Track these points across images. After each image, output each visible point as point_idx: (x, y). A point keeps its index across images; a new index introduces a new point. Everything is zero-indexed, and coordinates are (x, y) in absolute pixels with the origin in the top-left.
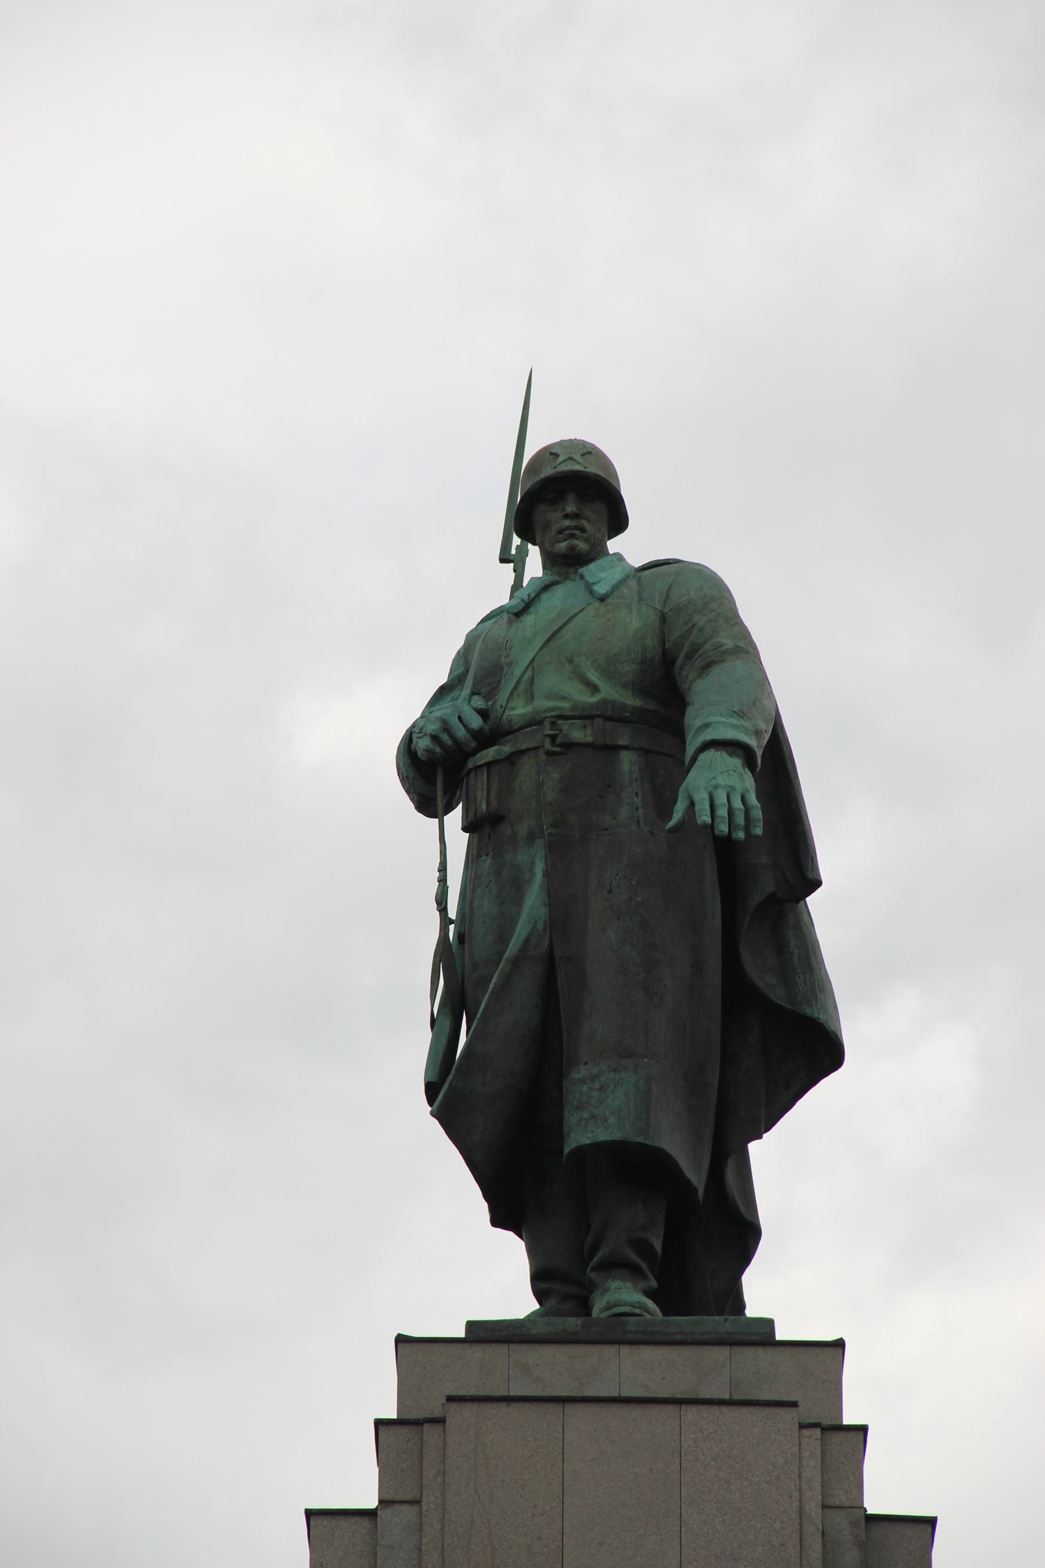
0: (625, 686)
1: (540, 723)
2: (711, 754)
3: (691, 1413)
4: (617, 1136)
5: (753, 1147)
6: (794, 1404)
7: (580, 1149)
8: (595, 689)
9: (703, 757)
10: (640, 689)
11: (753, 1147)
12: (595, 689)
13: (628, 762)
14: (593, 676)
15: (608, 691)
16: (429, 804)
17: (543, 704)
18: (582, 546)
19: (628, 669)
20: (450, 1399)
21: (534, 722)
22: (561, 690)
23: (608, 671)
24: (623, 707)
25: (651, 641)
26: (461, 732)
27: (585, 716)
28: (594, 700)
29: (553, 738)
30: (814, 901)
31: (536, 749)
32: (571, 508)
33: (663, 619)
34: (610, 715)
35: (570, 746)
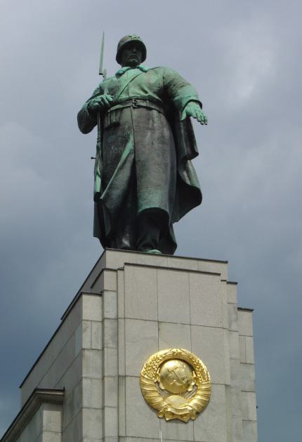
0: (154, 93)
1: (131, 100)
2: (192, 103)
3: (192, 274)
4: (157, 206)
5: (174, 225)
6: (219, 274)
7: (146, 210)
8: (146, 92)
9: (189, 104)
10: (157, 93)
11: (175, 225)
12: (146, 92)
13: (155, 113)
14: (146, 89)
15: (150, 93)
16: (85, 129)
17: (131, 95)
18: (136, 61)
19: (156, 89)
20: (126, 264)
21: (130, 99)
22: (135, 92)
23: (150, 88)
24: (154, 98)
25: (161, 83)
26: (107, 102)
27: (144, 99)
28: (147, 95)
29: (135, 104)
30: (195, 164)
31: (130, 107)
32: (134, 50)
33: (164, 78)
34: (151, 100)
35: (140, 107)
